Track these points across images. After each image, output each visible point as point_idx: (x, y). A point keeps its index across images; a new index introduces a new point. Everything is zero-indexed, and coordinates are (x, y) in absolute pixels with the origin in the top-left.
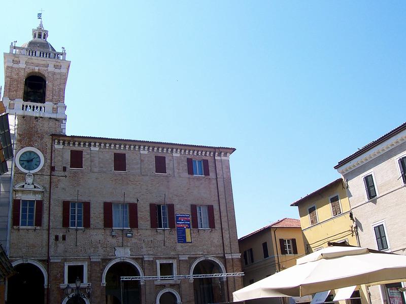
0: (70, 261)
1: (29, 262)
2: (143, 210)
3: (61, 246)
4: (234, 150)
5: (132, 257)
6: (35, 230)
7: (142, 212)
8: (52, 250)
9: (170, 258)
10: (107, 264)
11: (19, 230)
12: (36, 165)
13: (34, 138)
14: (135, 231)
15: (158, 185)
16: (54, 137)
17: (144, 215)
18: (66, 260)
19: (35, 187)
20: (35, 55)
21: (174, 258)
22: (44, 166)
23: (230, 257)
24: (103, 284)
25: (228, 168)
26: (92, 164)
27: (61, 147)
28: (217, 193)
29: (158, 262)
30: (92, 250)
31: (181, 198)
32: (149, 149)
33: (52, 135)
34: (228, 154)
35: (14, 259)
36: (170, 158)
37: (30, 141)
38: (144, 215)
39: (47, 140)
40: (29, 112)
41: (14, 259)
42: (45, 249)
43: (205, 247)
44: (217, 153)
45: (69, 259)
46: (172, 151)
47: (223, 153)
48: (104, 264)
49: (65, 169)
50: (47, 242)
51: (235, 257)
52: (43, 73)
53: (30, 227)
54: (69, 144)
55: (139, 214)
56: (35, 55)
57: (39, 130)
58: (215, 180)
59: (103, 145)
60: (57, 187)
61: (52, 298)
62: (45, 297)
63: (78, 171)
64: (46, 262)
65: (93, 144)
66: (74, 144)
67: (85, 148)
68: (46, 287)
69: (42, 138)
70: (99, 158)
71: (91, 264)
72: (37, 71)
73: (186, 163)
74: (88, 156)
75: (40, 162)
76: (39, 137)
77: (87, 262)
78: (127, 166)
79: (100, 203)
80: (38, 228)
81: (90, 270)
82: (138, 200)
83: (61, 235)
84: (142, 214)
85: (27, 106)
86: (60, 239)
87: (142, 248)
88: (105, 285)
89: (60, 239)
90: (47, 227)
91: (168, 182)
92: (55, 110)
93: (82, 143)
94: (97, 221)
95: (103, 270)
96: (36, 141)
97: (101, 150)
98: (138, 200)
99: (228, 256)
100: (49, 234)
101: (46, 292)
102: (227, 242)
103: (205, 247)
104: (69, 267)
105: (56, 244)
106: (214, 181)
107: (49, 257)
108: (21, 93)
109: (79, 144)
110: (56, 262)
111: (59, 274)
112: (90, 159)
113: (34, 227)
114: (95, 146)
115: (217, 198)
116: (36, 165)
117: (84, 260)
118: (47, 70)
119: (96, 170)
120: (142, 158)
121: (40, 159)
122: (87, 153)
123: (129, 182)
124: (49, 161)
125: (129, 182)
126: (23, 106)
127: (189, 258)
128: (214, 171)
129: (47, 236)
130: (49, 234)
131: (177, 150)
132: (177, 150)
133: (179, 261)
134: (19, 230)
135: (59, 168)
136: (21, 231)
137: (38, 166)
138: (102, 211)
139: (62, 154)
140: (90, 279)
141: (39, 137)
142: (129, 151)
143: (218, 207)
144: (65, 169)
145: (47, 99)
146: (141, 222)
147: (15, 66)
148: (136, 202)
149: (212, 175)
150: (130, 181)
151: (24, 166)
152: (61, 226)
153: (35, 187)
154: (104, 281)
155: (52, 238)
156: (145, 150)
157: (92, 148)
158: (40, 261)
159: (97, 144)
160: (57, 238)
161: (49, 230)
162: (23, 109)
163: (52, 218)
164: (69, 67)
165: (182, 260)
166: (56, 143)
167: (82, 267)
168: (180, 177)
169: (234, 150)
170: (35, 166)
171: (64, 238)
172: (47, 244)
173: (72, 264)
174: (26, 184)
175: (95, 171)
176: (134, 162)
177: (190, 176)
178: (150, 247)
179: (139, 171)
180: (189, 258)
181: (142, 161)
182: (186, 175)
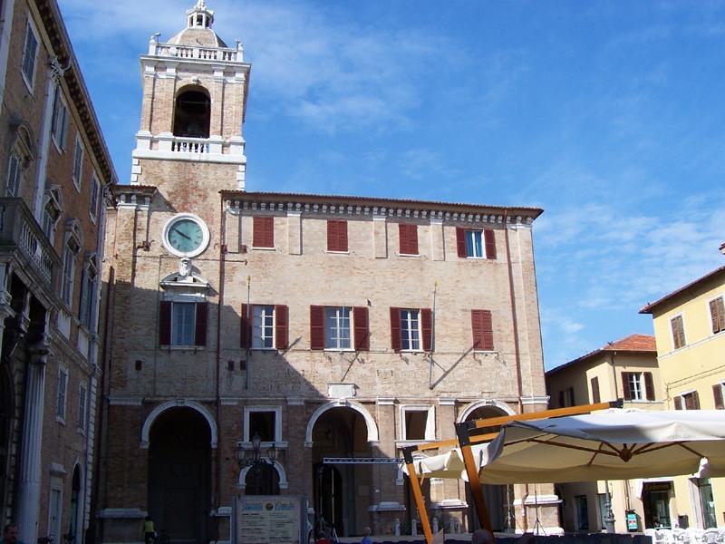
0: (254, 403)
1: (187, 404)
3: (238, 379)
4: (540, 212)
6: (196, 351)
7: (376, 322)
8: (223, 386)
11: (169, 351)
13: (192, 198)
14: (362, 355)
17: (380, 328)
18: (246, 403)
19: (195, 280)
24: (308, 443)
28: (509, 289)
29: (402, 408)
30: (290, 385)
34: (529, 219)
35: (162, 399)
37: (185, 204)
38: (380, 328)
39: (215, 199)
40: (184, 154)
42: (212, 384)
43: (485, 384)
44: (509, 218)
45: (251, 401)
47: (520, 218)
48: (310, 411)
50: (216, 371)
53: (187, 348)
54: (250, 206)
55: (372, 327)
57: (200, 184)
59: (307, 206)
60: (232, 281)
61: (224, 465)
62: (214, 463)
63: (265, 252)
64: (214, 405)
65: (290, 205)
66: (259, 207)
68: (213, 446)
69: (205, 198)
71: (289, 410)
73: (455, 237)
75: (201, 237)
76: (200, 195)
78: (350, 243)
79: (303, 307)
80: (201, 348)
81: (286, 419)
82: (369, 302)
83: (237, 361)
85: (179, 145)
87: (375, 384)
88: (311, 446)
90: (215, 348)
91: (422, 269)
93: (273, 205)
95: (308, 420)
96: (195, 202)
100: (218, 358)
101: (213, 455)
104: (253, 415)
105: (230, 376)
107: (218, 397)
109: (268, 207)
110: (231, 406)
111: (236, 425)
113: (193, 348)
117: (276, 403)
121: (202, 233)
123: (353, 270)
124: (217, 237)
125: (353, 270)
130: (218, 358)
131: (437, 213)
132: (437, 213)
134: (169, 351)
135: (232, 245)
136: (173, 355)
137: (198, 244)
138: (308, 319)
140: (286, 436)
141: (200, 195)
144: (243, 250)
146: (374, 341)
148: (366, 305)
149: (501, 256)
151: (176, 245)
152: (237, 346)
153: (195, 280)
154: (309, 439)
155: (224, 365)
156: (330, 214)
158: (204, 403)
159: (298, 205)
160: (231, 366)
161: (218, 352)
162: (173, 149)
163: (223, 332)
167: (273, 414)
169: (540, 212)
170: (194, 245)
171: (243, 366)
172: (215, 375)
173: (256, 410)
176: (363, 235)
177: (463, 260)
178: (390, 383)
182: (453, 255)
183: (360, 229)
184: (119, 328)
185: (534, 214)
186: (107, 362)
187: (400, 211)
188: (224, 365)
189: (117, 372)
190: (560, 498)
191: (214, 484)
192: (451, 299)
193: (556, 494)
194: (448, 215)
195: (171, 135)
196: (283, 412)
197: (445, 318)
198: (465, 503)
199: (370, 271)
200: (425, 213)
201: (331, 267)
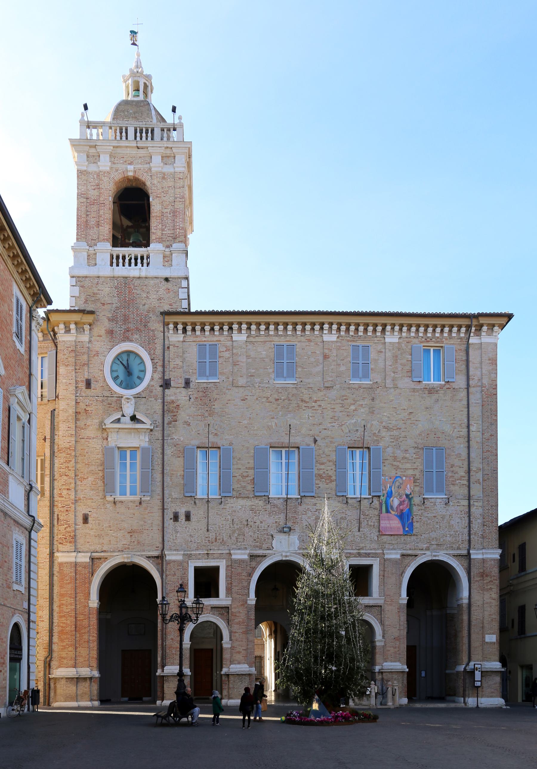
0: (198, 557)
2: (325, 461)
4: (510, 317)
5: (301, 551)
7: (323, 464)
9: (367, 555)
10: (259, 563)
12: (139, 378)
15: (353, 407)
16: (168, 319)
18: (190, 556)
20: (127, 139)
21: (375, 555)
22: (152, 379)
23: (480, 557)
25: (494, 362)
26: (236, 369)
27: (180, 337)
31: (395, 433)
32: (339, 329)
33: (165, 314)
34: (496, 328)
36: (380, 347)
39: (156, 325)
41: (109, 554)
44: (473, 329)
45: (195, 555)
46: (384, 330)
47: (485, 328)
48: (254, 564)
49: (187, 383)
51: (489, 556)
52: (143, 179)
56: (127, 139)
58: (466, 391)
65: (235, 327)
67: (222, 339)
70: (248, 357)
71: (232, 565)
72: (131, 174)
74: (227, 354)
77: (225, 560)
82: (315, 441)
84: (322, 467)
86: (182, 517)
89: (182, 517)
91: (373, 399)
92: (167, 259)
94: (243, 484)
95: (250, 575)
97: (251, 339)
98: (315, 441)
99: (476, 555)
102: (476, 526)
103: (433, 535)
106: (464, 394)
108: (107, 229)
112: (231, 360)
114: (240, 330)
115: (464, 431)
116: (139, 378)
118: (150, 169)
119: (242, 381)
120: (326, 351)
122: (226, 347)
124: (160, 369)
126: (112, 257)
127: (403, 555)
128: (465, 371)
129: (161, 514)
132: (393, 329)
133: (384, 562)
139: (183, 353)
140: (229, 590)
142: (303, 339)
143: (466, 450)
145: (153, 237)
147: (93, 168)
150: (302, 401)
151: (119, 381)
155: (169, 515)
157: (236, 336)
160: (176, 518)
162: (111, 265)
164: (190, 156)
165: (389, 560)
166: (171, 332)
168: (396, 387)
169: (510, 317)
170: (137, 381)
171: (188, 517)
174: (123, 416)
175: (240, 384)
176: (312, 359)
179: (320, 379)
180: (403, 555)
181: (326, 357)
183: (310, 353)
184: (65, 478)
185: (503, 321)
186: (56, 517)
187: (352, 328)
188: (169, 515)
189: (66, 526)
190: (503, 666)
191: (159, 642)
192: (403, 434)
193: (500, 662)
194: (405, 329)
195: (108, 246)
196: (227, 566)
197: (395, 458)
198: (405, 667)
199: (318, 403)
200: (379, 328)
201: (277, 400)
